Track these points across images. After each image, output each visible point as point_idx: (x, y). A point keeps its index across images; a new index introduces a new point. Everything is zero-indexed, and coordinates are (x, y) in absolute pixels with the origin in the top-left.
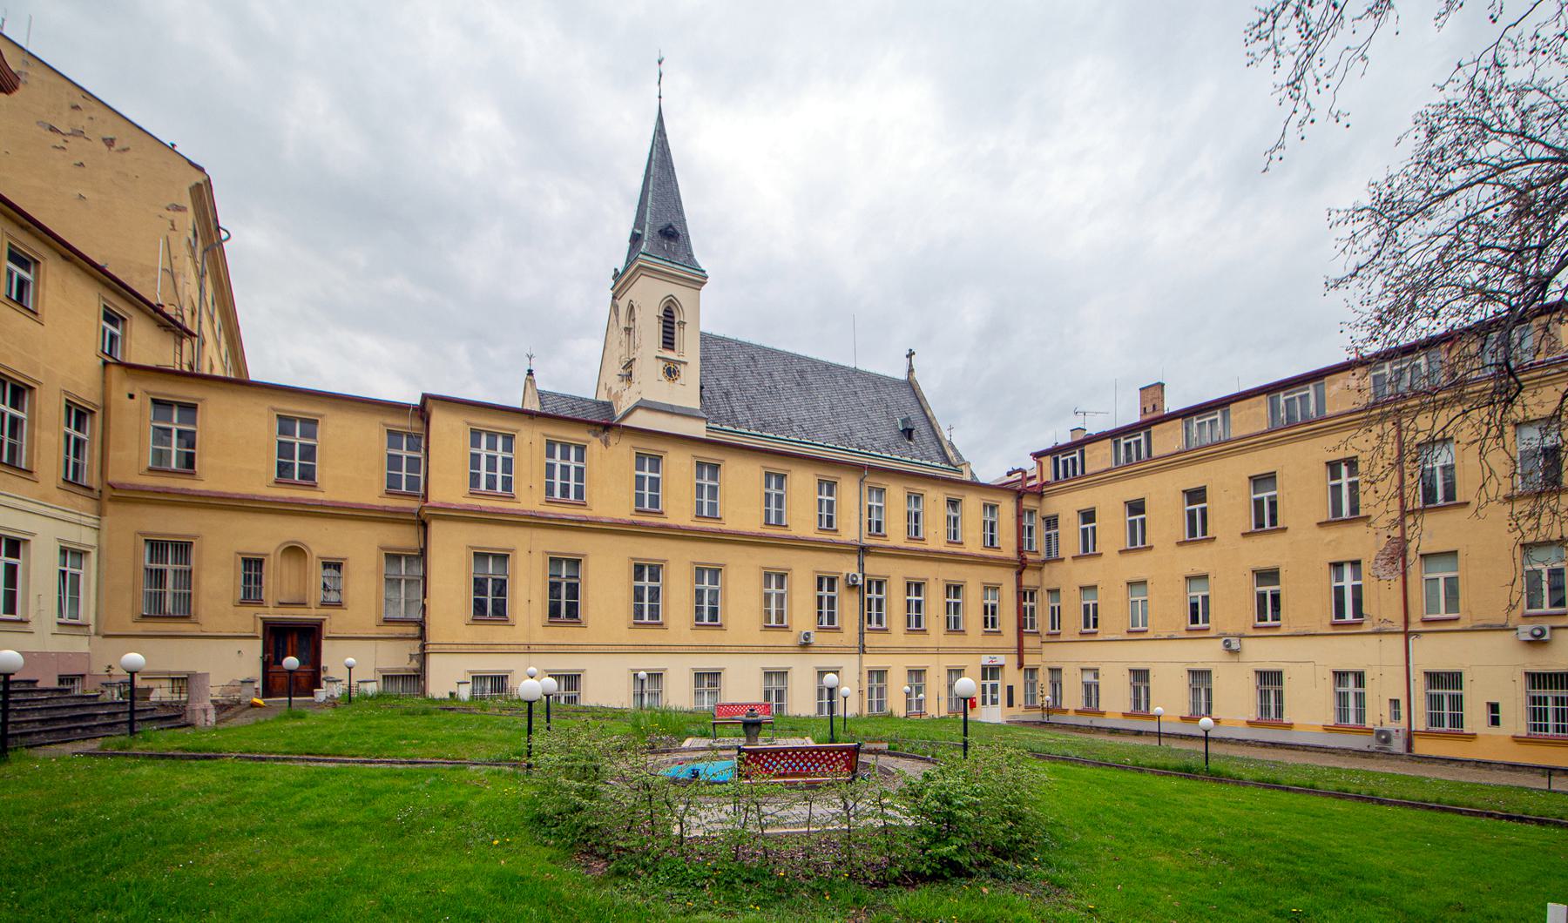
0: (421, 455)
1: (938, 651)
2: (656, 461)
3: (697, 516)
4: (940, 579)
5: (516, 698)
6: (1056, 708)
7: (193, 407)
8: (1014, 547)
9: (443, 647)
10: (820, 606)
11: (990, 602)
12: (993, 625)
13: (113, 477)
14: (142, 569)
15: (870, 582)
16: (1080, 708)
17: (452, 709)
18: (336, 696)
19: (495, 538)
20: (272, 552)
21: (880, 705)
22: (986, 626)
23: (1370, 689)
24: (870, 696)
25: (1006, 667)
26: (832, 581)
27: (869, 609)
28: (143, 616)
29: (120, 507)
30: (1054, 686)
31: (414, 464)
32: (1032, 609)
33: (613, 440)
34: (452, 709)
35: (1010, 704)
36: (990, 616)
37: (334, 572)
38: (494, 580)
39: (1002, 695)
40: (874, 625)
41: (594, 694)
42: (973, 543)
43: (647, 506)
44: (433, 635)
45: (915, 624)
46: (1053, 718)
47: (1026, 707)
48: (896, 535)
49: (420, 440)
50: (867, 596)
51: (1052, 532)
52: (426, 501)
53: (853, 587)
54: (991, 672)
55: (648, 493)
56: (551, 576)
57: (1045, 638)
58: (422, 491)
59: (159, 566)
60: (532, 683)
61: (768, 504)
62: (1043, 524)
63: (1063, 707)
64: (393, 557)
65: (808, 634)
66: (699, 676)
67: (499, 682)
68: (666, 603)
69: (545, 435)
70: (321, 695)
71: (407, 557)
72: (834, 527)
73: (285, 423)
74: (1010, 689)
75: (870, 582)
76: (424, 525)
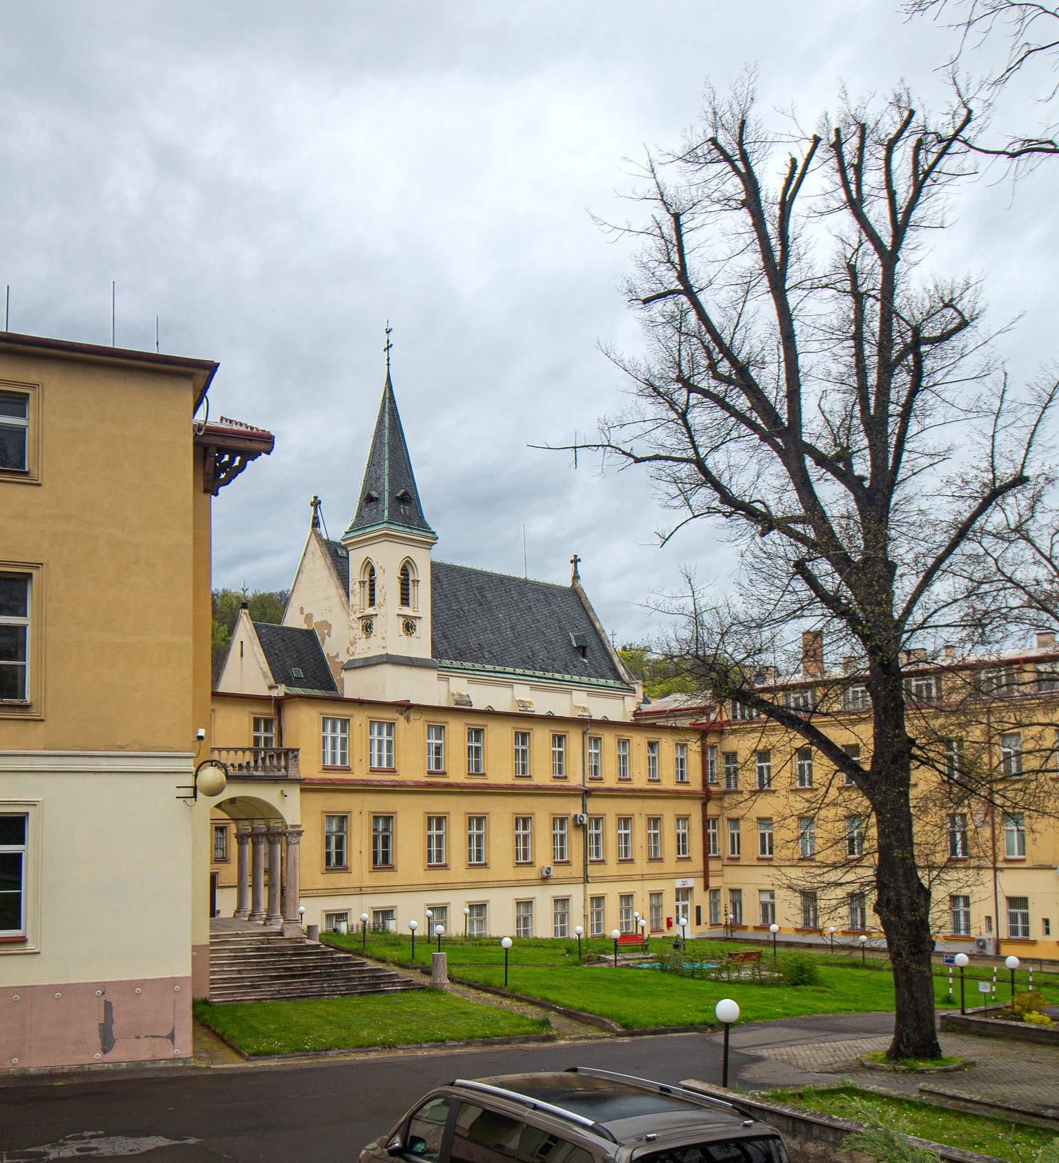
1: (643, 878)
4: (643, 815)
6: (735, 925)
8: (700, 780)
11: (681, 831)
16: (758, 925)
23: (973, 909)
25: (695, 890)
26: (562, 821)
32: (714, 835)
35: (699, 923)
39: (691, 913)
42: (668, 782)
47: (711, 925)
50: (589, 832)
53: (580, 826)
54: (684, 893)
57: (726, 862)
63: (744, 924)
74: (698, 908)
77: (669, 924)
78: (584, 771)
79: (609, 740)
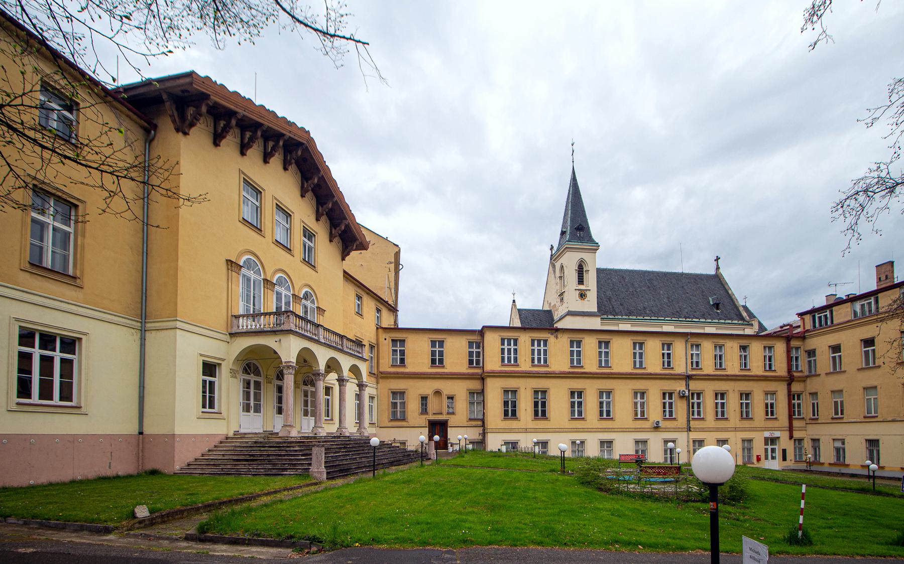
0: (480, 350)
1: (736, 430)
2: (579, 343)
3: (599, 367)
4: (736, 390)
6: (817, 462)
7: (404, 341)
10: (664, 407)
11: (769, 401)
12: (772, 414)
13: (381, 370)
15: (693, 394)
19: (511, 383)
20: (430, 393)
22: (767, 414)
26: (671, 395)
27: (693, 407)
29: (384, 380)
30: (815, 449)
31: (478, 354)
32: (799, 405)
33: (559, 336)
35: (784, 459)
36: (769, 409)
37: (451, 400)
38: (511, 401)
39: (778, 454)
40: (696, 416)
41: (553, 451)
45: (721, 415)
46: (813, 468)
47: (795, 462)
48: (708, 367)
49: (480, 344)
50: (691, 401)
51: (812, 359)
53: (682, 396)
54: (773, 441)
55: (576, 356)
56: (534, 398)
57: (808, 421)
58: (481, 365)
59: (395, 401)
61: (635, 357)
62: (806, 355)
64: (472, 393)
65: (658, 422)
66: (602, 443)
67: (514, 445)
68: (585, 409)
69: (530, 337)
71: (477, 393)
72: (672, 366)
73: (433, 343)
74: (784, 451)
75: (693, 394)
76: (483, 379)
77: (759, 459)
78: (686, 364)
79: (707, 346)
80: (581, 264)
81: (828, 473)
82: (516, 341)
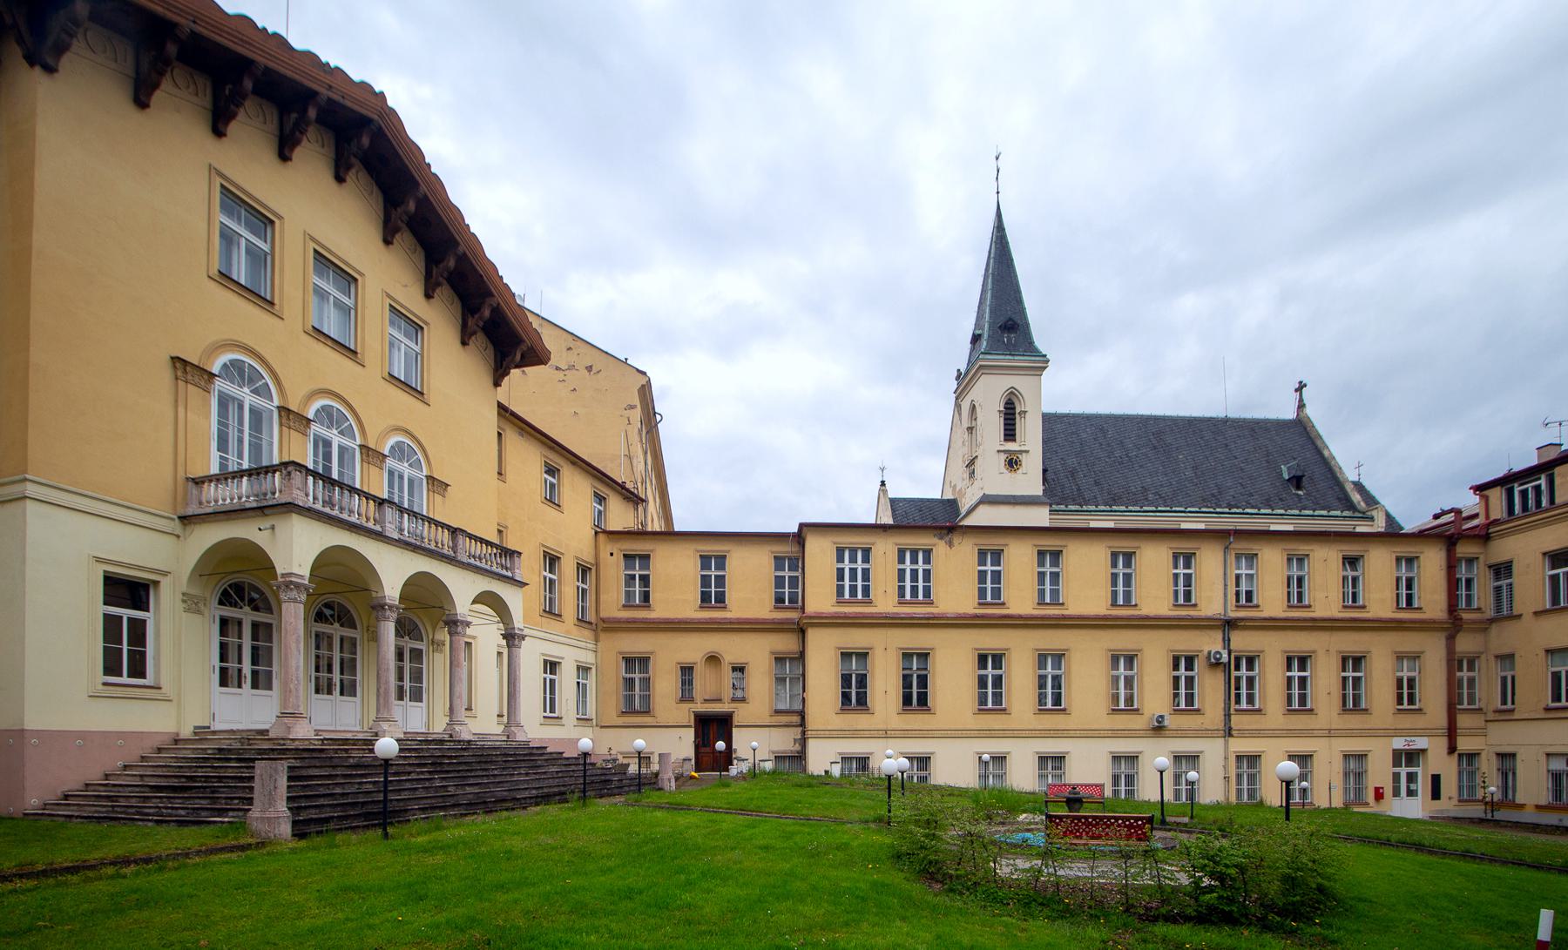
1: (1330, 733)
2: (997, 556)
3: (1039, 604)
5: (876, 776)
6: (1507, 801)
7: (647, 557)
9: (819, 732)
13: (603, 614)
14: (621, 679)
15: (1238, 659)
17: (828, 784)
18: (744, 771)
19: (857, 639)
21: (1252, 793)
22: (1400, 701)
24: (1239, 782)
25: (1429, 751)
26: (1190, 662)
27: (1238, 688)
28: (623, 712)
29: (608, 635)
30: (1505, 775)
31: (794, 582)
32: (1471, 681)
33: (956, 540)
34: (828, 784)
35: (1436, 794)
36: (1405, 691)
37: (739, 675)
39: (1423, 785)
40: (1244, 705)
43: (989, 599)
44: (813, 722)
45: (1299, 700)
46: (1498, 815)
47: (1460, 801)
48: (1272, 602)
49: (798, 562)
50: (1234, 673)
51: (1503, 583)
52: (804, 613)
54: (1411, 757)
55: (990, 584)
56: (903, 669)
57: (1491, 716)
60: (890, 760)
61: (1114, 583)
62: (1490, 575)
63: (1517, 801)
65: (1162, 717)
68: (1009, 690)
70: (734, 770)
71: (791, 659)
72: (1193, 602)
73: (705, 561)
74: (1436, 780)
75: (1238, 659)
77: (1379, 795)
80: (1010, 399)
81: (1535, 828)
82: (867, 553)
